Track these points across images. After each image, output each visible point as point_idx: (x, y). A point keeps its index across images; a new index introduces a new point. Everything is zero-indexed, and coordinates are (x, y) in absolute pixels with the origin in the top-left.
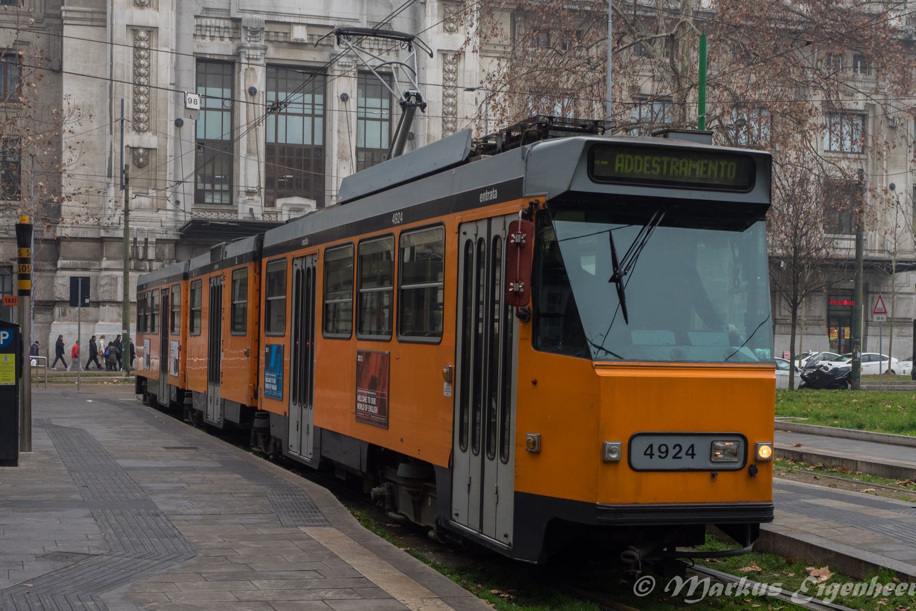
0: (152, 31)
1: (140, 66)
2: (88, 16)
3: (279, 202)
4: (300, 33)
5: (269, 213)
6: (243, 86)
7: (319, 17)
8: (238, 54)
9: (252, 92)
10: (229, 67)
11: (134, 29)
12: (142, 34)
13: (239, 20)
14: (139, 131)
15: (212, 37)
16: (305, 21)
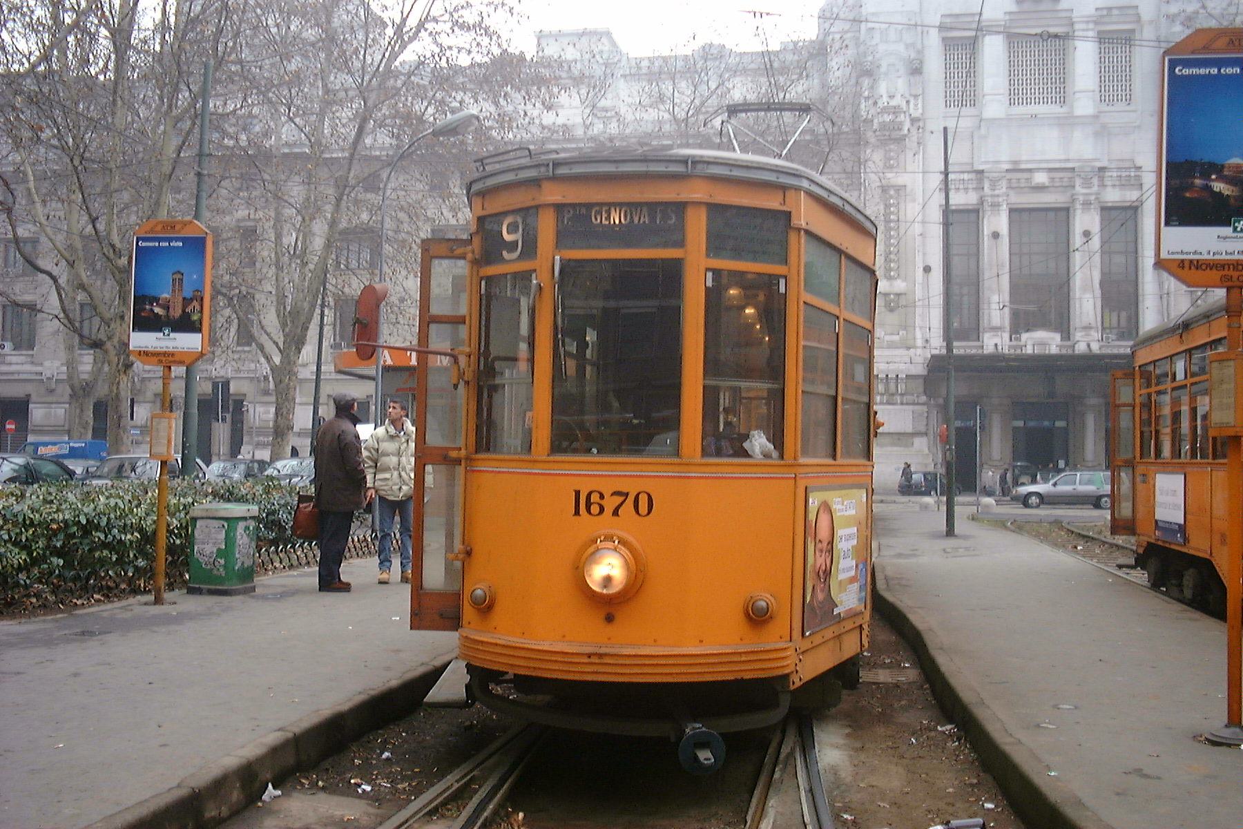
0: (900, 189)
1: (890, 221)
3: (1025, 336)
4: (1041, 178)
5: (1015, 348)
6: (987, 231)
7: (1060, 161)
8: (982, 201)
9: (996, 235)
10: (973, 217)
12: (892, 192)
13: (982, 172)
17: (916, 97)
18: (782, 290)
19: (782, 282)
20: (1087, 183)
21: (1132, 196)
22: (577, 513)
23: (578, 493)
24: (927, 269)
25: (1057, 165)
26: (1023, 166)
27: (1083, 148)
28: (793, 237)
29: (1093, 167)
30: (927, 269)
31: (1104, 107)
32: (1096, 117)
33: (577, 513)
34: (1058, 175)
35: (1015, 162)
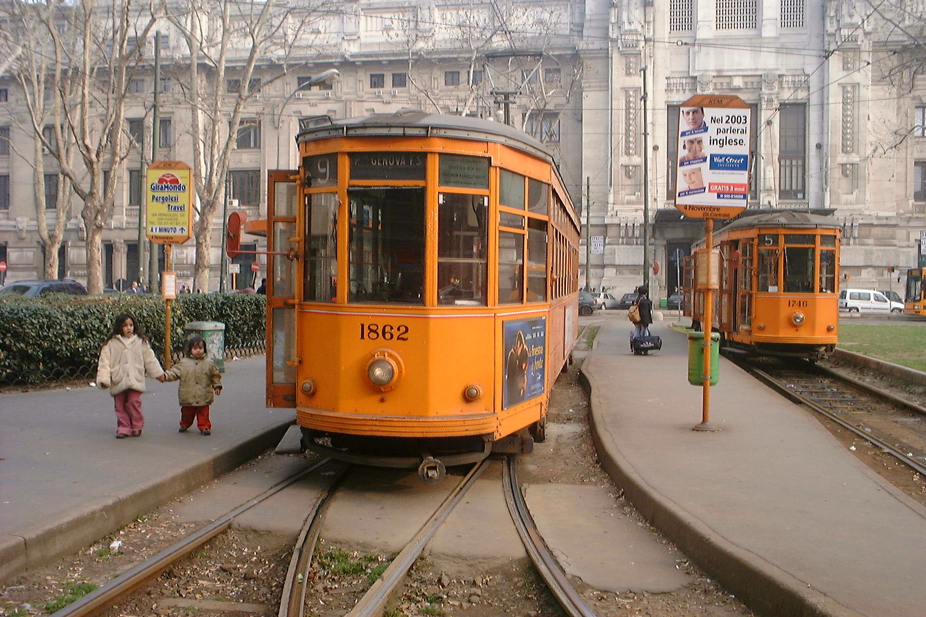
2: (598, 84)
7: (751, 70)
11: (626, 90)
14: (628, 154)
15: (678, 90)
16: (741, 73)
17: (649, 23)
18: (486, 204)
19: (486, 199)
20: (770, 85)
21: (801, 95)
22: (362, 337)
23: (363, 326)
24: (656, 148)
25: (749, 73)
26: (725, 74)
27: (768, 62)
28: (492, 170)
29: (774, 76)
30: (656, 148)
31: (785, 31)
32: (777, 38)
33: (362, 337)
34: (749, 80)
35: (719, 71)
